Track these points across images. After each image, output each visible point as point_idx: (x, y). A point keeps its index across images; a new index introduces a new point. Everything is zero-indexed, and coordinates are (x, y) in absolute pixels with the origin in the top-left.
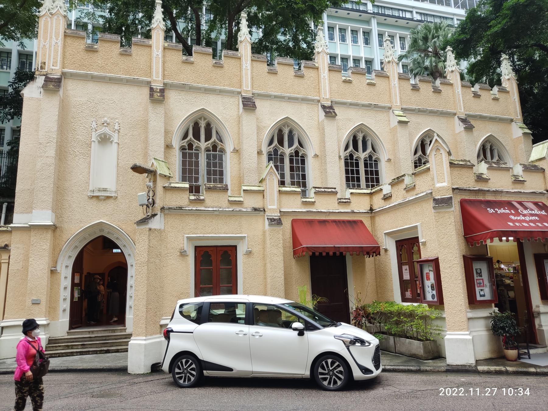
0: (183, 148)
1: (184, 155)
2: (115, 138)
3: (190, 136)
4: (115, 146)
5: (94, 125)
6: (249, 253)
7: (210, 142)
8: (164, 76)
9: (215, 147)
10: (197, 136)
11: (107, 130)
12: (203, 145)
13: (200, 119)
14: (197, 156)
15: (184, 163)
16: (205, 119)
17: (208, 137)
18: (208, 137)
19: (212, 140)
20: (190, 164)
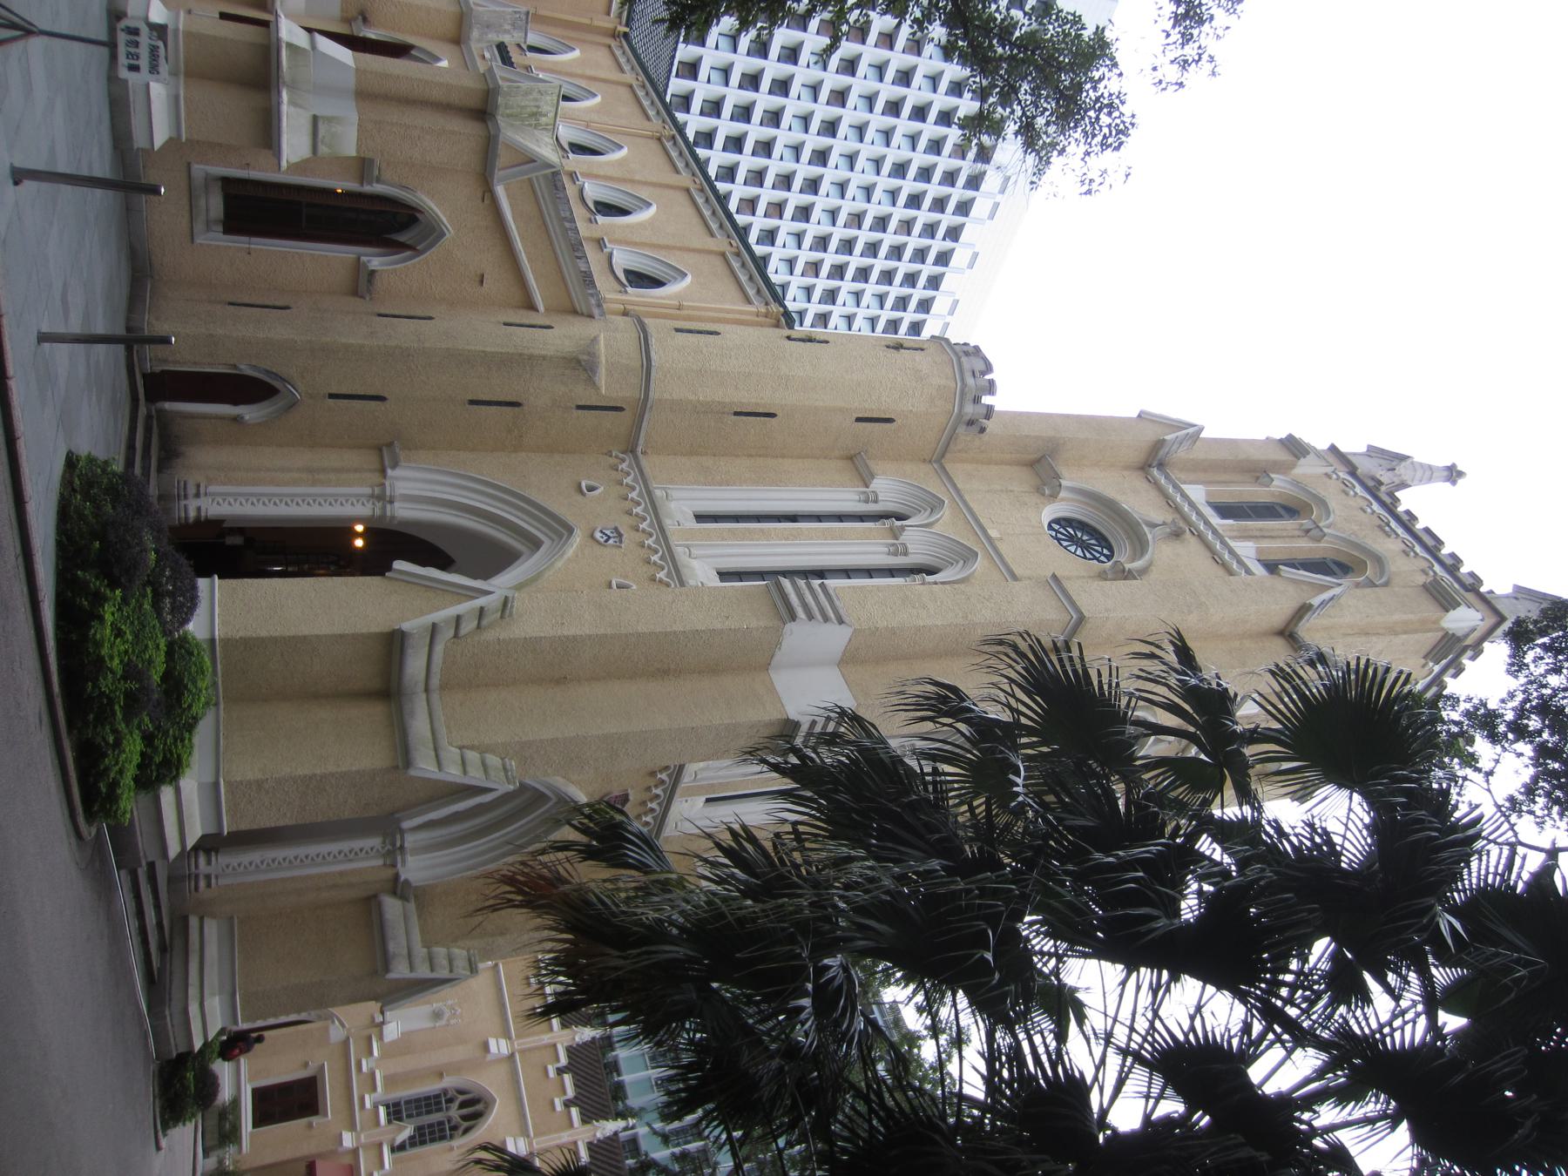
0: (445, 1092)
1: (437, 1096)
2: (443, 1022)
3: (461, 1098)
4: (431, 1025)
5: (450, 1002)
6: (310, 1126)
7: (459, 1120)
8: (522, 1052)
9: (454, 1128)
10: (463, 1105)
11: (447, 1014)
12: (454, 1113)
13: (486, 1103)
14: (440, 1110)
15: (427, 1098)
16: (486, 1108)
17: (465, 1118)
18: (465, 1118)
19: (462, 1122)
20: (429, 1105)
